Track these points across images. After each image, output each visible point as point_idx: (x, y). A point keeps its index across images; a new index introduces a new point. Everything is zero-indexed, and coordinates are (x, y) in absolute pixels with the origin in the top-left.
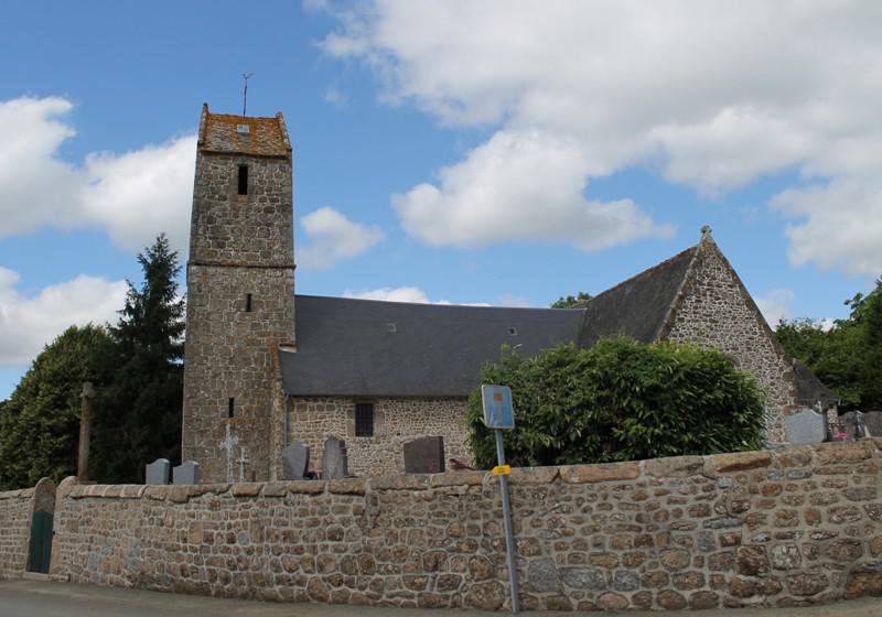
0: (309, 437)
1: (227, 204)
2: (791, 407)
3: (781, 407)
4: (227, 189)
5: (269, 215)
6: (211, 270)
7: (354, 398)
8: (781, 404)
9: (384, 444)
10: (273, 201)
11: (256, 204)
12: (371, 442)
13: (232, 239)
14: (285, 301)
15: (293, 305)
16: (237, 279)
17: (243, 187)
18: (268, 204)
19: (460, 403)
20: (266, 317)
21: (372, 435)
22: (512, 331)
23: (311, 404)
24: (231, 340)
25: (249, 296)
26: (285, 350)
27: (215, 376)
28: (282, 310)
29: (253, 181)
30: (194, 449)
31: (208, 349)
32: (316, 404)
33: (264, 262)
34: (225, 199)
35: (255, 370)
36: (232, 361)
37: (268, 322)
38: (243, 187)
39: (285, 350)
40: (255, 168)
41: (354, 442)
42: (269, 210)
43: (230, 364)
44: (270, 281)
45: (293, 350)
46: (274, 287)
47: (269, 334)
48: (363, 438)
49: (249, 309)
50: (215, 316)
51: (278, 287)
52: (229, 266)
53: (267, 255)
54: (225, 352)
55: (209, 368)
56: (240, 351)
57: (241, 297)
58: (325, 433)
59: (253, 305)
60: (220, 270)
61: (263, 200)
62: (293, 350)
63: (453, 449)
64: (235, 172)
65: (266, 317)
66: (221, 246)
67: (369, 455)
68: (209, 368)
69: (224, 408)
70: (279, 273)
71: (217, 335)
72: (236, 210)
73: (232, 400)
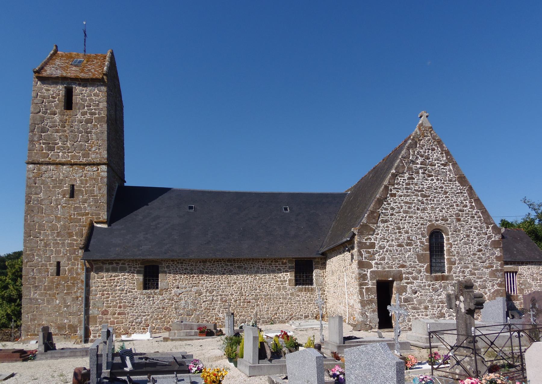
0: (105, 290)
1: (57, 118)
2: (497, 270)
3: (488, 271)
4: (56, 106)
5: (89, 125)
6: (44, 168)
7: (143, 262)
8: (487, 268)
9: (166, 295)
10: (92, 114)
11: (79, 116)
12: (155, 294)
13: (60, 144)
14: (100, 189)
15: (105, 192)
16: (63, 174)
17: (69, 104)
18: (88, 116)
19: (229, 264)
20: (85, 201)
21: (157, 288)
22: (286, 209)
23: (107, 266)
24: (58, 219)
25: (73, 186)
26: (99, 225)
27: (46, 245)
28: (97, 196)
29: (77, 99)
30: (30, 299)
31: (41, 227)
32: (111, 266)
33: (84, 160)
34: (55, 114)
35: (77, 241)
36: (59, 234)
37: (86, 205)
38: (69, 104)
39: (99, 225)
40: (77, 89)
41: (142, 294)
42: (89, 121)
43: (58, 236)
44: (88, 175)
45: (105, 226)
46: (91, 179)
47: (88, 214)
48: (149, 291)
49: (72, 195)
50: (46, 202)
51: (94, 179)
52: (57, 164)
53: (86, 155)
54: (53, 228)
55: (41, 240)
56: (64, 227)
57: (66, 188)
58: (118, 288)
59: (76, 193)
60: (52, 167)
61: (84, 114)
62: (105, 226)
63: (222, 298)
64: (62, 93)
65: (85, 201)
66: (52, 149)
67: (154, 303)
68: (41, 240)
69: (52, 269)
70: (95, 168)
71: (48, 215)
72: (63, 123)
73: (58, 263)
